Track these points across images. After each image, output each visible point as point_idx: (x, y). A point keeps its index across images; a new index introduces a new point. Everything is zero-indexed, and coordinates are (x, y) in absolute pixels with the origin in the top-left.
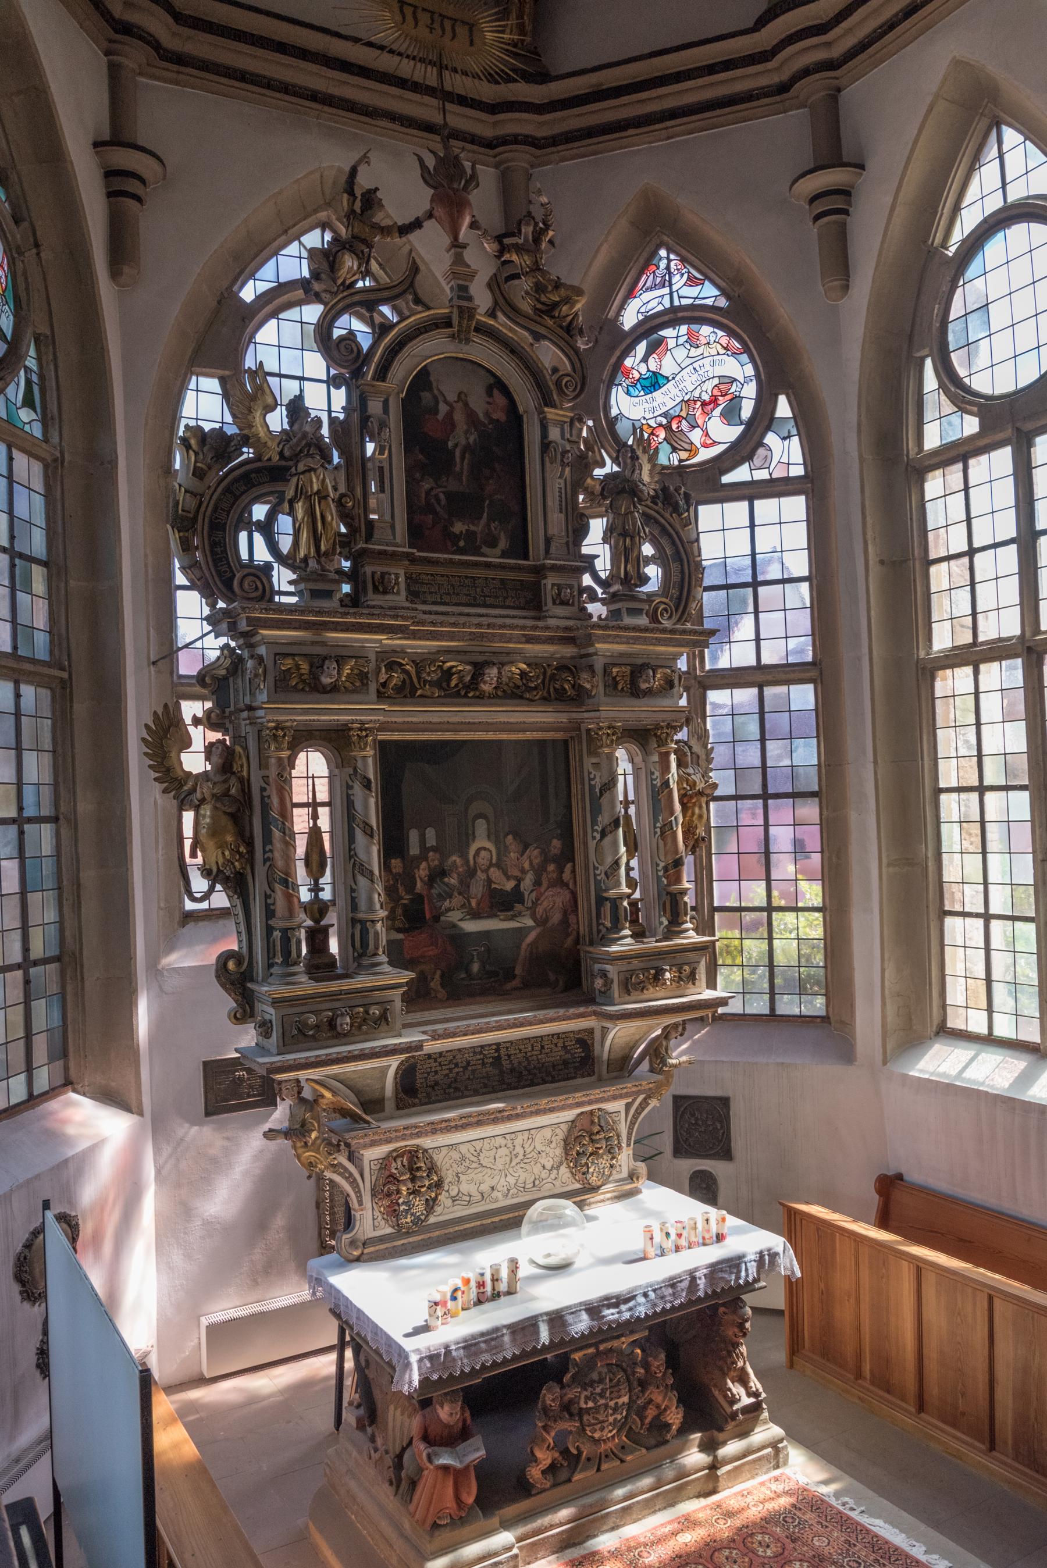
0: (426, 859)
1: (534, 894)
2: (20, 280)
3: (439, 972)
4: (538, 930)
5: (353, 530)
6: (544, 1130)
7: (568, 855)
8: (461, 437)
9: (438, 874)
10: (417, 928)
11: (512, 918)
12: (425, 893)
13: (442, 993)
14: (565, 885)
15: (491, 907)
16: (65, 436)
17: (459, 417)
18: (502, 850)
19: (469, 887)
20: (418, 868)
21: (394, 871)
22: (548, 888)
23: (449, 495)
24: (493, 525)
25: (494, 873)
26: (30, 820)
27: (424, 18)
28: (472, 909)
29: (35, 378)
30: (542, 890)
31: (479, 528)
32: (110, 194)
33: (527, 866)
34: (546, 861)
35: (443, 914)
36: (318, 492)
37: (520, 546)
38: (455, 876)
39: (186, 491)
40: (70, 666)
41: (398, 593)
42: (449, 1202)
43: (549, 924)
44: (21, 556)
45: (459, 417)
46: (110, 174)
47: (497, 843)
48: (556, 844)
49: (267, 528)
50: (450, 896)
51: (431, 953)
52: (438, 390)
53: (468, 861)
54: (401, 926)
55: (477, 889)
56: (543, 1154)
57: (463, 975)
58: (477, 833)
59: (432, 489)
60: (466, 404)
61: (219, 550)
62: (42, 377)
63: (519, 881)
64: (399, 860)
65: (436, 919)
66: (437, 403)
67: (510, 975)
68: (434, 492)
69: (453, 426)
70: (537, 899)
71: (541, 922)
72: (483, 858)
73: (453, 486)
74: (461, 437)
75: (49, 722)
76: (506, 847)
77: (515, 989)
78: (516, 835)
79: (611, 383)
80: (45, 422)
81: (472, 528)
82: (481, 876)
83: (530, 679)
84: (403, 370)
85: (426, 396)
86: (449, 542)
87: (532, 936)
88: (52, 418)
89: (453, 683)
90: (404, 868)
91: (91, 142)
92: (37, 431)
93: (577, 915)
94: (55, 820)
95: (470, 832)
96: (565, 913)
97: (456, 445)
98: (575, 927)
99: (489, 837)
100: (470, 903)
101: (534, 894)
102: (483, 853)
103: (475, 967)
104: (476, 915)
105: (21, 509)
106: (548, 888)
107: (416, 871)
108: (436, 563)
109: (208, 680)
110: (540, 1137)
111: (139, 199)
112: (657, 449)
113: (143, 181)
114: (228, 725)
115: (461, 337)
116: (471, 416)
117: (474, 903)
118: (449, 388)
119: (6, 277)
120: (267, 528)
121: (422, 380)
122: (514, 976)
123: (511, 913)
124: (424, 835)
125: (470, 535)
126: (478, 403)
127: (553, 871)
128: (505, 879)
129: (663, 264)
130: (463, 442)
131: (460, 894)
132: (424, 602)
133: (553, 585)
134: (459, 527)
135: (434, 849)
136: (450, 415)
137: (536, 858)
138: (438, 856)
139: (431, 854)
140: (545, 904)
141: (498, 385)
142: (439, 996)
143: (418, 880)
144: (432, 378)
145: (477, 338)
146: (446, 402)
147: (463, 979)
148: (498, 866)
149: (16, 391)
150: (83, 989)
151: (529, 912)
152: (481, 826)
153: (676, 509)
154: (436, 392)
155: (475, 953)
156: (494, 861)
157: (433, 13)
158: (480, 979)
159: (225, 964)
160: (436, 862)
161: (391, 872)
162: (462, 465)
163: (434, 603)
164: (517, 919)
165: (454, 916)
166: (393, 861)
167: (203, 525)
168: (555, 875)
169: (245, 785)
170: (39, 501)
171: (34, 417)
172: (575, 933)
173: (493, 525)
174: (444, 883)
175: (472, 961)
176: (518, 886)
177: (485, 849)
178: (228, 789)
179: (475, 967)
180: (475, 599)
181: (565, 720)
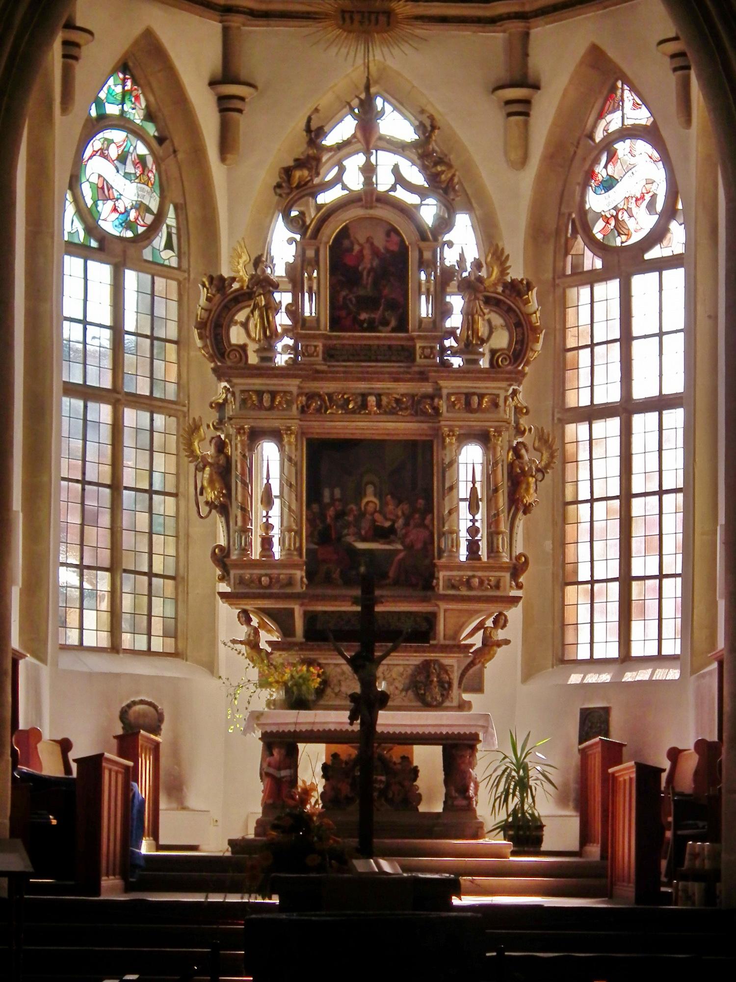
2: (164, 178)
3: (339, 570)
6: (398, 668)
7: (429, 509)
8: (368, 263)
11: (389, 543)
13: (340, 582)
14: (426, 527)
16: (192, 263)
17: (367, 252)
18: (384, 504)
23: (358, 298)
24: (386, 314)
25: (377, 516)
26: (158, 493)
27: (357, 17)
29: (174, 231)
31: (377, 315)
33: (400, 513)
36: (265, 305)
37: (402, 325)
39: (202, 309)
40: (189, 403)
41: (317, 356)
42: (333, 695)
44: (158, 339)
45: (367, 252)
46: (222, 99)
47: (380, 499)
48: (421, 502)
52: (355, 238)
53: (360, 508)
55: (365, 525)
56: (396, 681)
59: (347, 295)
60: (372, 244)
61: (219, 337)
62: (178, 229)
63: (394, 522)
65: (339, 539)
66: (352, 244)
67: (385, 576)
68: (348, 297)
69: (363, 256)
71: (409, 547)
72: (371, 508)
73: (361, 292)
74: (368, 263)
75: (175, 437)
78: (393, 496)
80: (179, 256)
81: (373, 316)
82: (368, 517)
83: (403, 403)
84: (331, 232)
85: (346, 243)
87: (401, 555)
88: (185, 253)
89: (351, 406)
91: (207, 81)
92: (174, 263)
94: (175, 495)
96: (425, 544)
97: (364, 268)
101: (404, 531)
102: (371, 505)
103: (362, 569)
104: (364, 540)
105: (160, 311)
108: (343, 338)
109: (213, 405)
111: (240, 111)
112: (508, 256)
113: (242, 99)
114: (224, 429)
116: (375, 252)
117: (363, 532)
118: (361, 236)
119: (154, 176)
120: (245, 325)
121: (344, 233)
126: (380, 242)
129: (619, 92)
130: (369, 266)
131: (355, 526)
132: (338, 361)
133: (420, 347)
134: (364, 316)
135: (340, 500)
136: (361, 251)
140: (412, 537)
141: (392, 231)
144: (351, 231)
145: (379, 205)
146: (360, 244)
148: (380, 512)
149: (160, 241)
150: (187, 598)
152: (370, 489)
154: (352, 239)
157: (363, 12)
159: (215, 551)
162: (367, 280)
163: (344, 361)
165: (350, 539)
169: (228, 459)
170: (174, 306)
171: (174, 254)
173: (386, 314)
176: (392, 526)
178: (219, 461)
179: (362, 569)
180: (370, 357)
181: (426, 428)
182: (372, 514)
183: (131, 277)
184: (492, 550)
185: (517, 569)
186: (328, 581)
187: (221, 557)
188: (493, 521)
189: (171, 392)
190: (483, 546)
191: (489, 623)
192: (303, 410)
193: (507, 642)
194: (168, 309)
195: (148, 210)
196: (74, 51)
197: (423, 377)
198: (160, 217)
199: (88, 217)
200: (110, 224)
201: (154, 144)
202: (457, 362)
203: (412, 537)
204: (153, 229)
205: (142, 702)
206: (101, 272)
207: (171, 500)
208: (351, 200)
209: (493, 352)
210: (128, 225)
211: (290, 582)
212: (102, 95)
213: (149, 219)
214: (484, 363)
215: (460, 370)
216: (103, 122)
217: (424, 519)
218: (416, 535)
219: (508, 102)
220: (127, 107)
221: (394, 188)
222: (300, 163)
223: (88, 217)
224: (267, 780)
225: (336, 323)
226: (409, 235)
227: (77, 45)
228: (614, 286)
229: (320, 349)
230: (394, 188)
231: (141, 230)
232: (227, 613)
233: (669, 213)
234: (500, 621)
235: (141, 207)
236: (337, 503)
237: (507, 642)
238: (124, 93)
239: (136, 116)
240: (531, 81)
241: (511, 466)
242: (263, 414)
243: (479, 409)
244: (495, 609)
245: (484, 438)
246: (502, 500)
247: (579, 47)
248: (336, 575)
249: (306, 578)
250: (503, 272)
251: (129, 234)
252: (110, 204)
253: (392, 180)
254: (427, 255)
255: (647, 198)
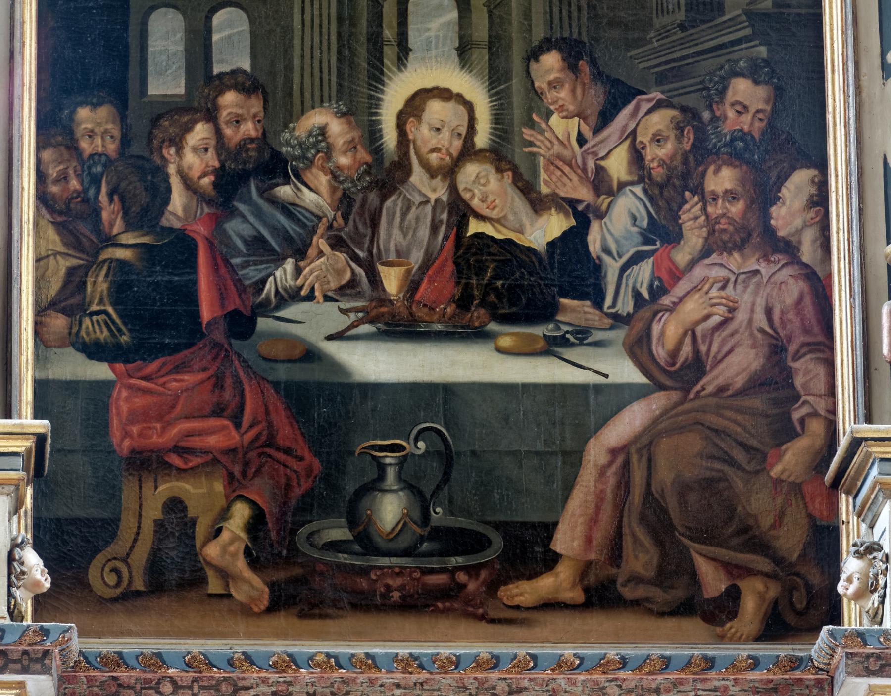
0: (211, 115)
1: (644, 272)
3: (241, 512)
4: (658, 402)
10: (163, 350)
12: (200, 230)
15: (464, 303)
19: (374, 224)
20: (178, 143)
21: (85, 145)
22: (706, 253)
28: (383, 300)
30: (681, 257)
35: (264, 308)
38: (322, 180)
43: (710, 382)
50: (300, 252)
51: (212, 441)
53: (373, 135)
54: (103, 335)
57: (339, 533)
58: (414, 39)
64: (104, 112)
70: (658, 291)
76: (534, 94)
77: (550, 606)
90: (125, 141)
93: (830, 364)
95: (389, 33)
98: (821, 406)
99: (464, 51)
100: (375, 280)
101: (644, 272)
102: (436, 109)
106: (706, 253)
107: (170, 152)
122: (551, 560)
123: (539, 330)
124: (209, 31)
127: (731, 196)
128: (520, 204)
131: (337, 243)
137: (658, 139)
138: (256, 105)
139: (229, 99)
140: (692, 309)
142: (239, 594)
143: (176, 183)
147: (335, 546)
151: (619, 334)
155: (390, 459)
156: (482, 139)
158: (407, 553)
160: (249, 129)
161: (73, 147)
164: (570, 354)
166: (83, 113)
168: (736, 209)
172: (816, 427)
174: (274, 202)
175: (375, 485)
177: (445, 94)
182: (450, 172)
203: (692, 309)
236: (229, 99)
249: (38, 547)
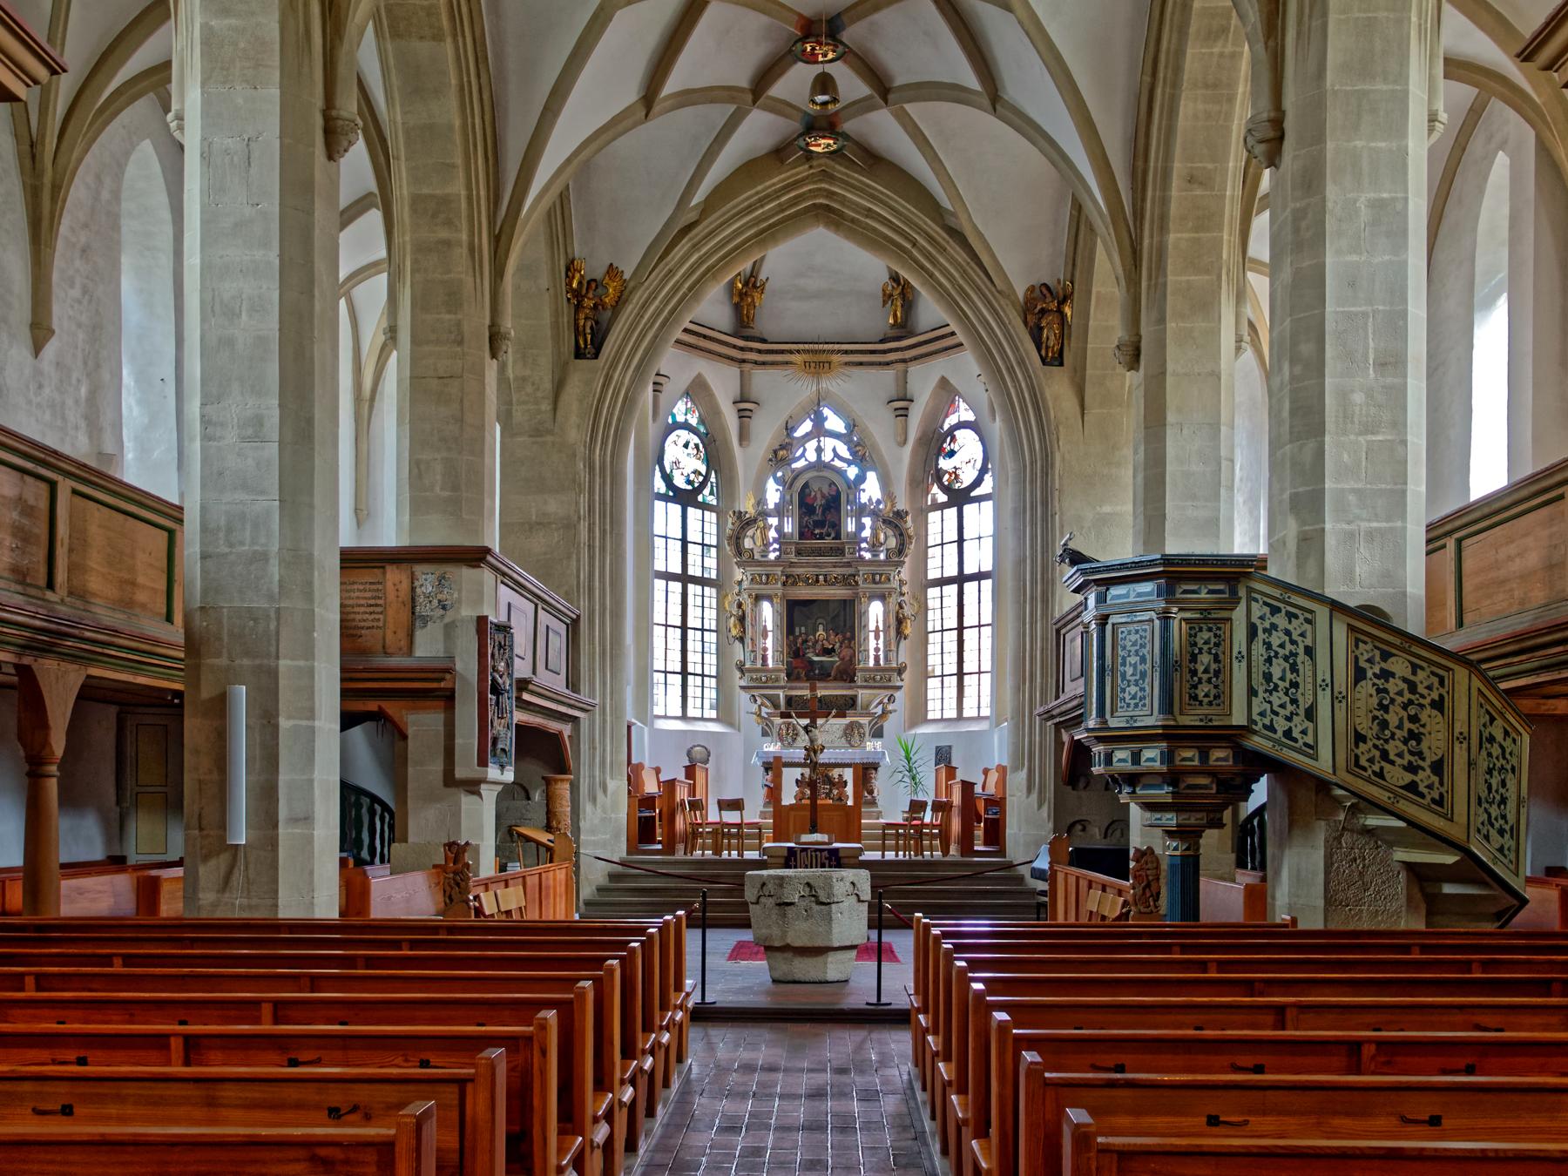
5: (780, 536)
7: (853, 637)
8: (819, 502)
9: (805, 641)
17: (819, 496)
31: (824, 531)
32: (740, 417)
34: (845, 638)
37: (838, 537)
44: (707, 545)
45: (819, 496)
49: (753, 537)
55: (818, 647)
62: (717, 483)
71: (842, 659)
73: (816, 518)
74: (819, 502)
79: (938, 455)
80: (718, 499)
85: (807, 490)
86: (814, 536)
92: (714, 502)
96: (851, 657)
103: (817, 672)
104: (818, 655)
110: (835, 728)
111: (750, 417)
113: (751, 411)
115: (819, 470)
116: (823, 496)
118: (815, 487)
121: (806, 485)
125: (821, 534)
126: (826, 490)
134: (817, 531)
141: (832, 483)
149: (706, 491)
152: (821, 627)
153: (902, 518)
165: (810, 655)
167: (734, 539)
176: (833, 648)
179: (817, 672)
183: (691, 510)
184: (887, 659)
185: (900, 671)
186: (798, 679)
187: (741, 668)
188: (887, 643)
189: (714, 576)
190: (882, 657)
191: (886, 700)
192: (784, 584)
193: (895, 711)
194: (712, 528)
195: (700, 474)
196: (658, 387)
197: (848, 564)
198: (707, 478)
199: (667, 478)
200: (679, 482)
201: (704, 437)
202: (867, 556)
204: (703, 485)
205: (699, 746)
206: (676, 509)
207: (714, 635)
208: (811, 467)
209: (887, 550)
210: (689, 482)
211: (777, 680)
212: (675, 411)
213: (701, 478)
214: (882, 557)
215: (869, 561)
216: (677, 426)
217: (850, 642)
218: (846, 652)
219: (896, 409)
220: (689, 416)
221: (833, 460)
222: (782, 447)
223: (667, 478)
224: (766, 788)
225: (802, 535)
226: (842, 486)
227: (661, 384)
228: (954, 510)
229: (793, 550)
230: (833, 460)
231: (696, 485)
232: (744, 697)
233: (983, 471)
234: (891, 699)
235: (696, 472)
237: (895, 711)
238: (687, 409)
239: (693, 421)
240: (908, 397)
241: (898, 613)
242: (763, 586)
243: (880, 582)
244: (889, 692)
245: (883, 598)
246: (893, 633)
247: (934, 381)
248: (803, 675)
250: (893, 505)
251: (690, 487)
252: (680, 471)
253: (832, 455)
254: (851, 497)
255: (972, 462)
